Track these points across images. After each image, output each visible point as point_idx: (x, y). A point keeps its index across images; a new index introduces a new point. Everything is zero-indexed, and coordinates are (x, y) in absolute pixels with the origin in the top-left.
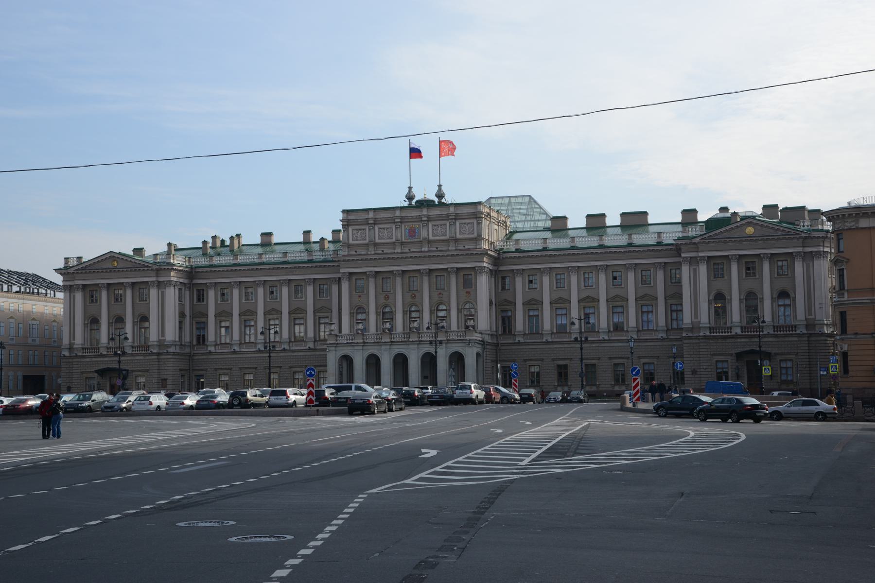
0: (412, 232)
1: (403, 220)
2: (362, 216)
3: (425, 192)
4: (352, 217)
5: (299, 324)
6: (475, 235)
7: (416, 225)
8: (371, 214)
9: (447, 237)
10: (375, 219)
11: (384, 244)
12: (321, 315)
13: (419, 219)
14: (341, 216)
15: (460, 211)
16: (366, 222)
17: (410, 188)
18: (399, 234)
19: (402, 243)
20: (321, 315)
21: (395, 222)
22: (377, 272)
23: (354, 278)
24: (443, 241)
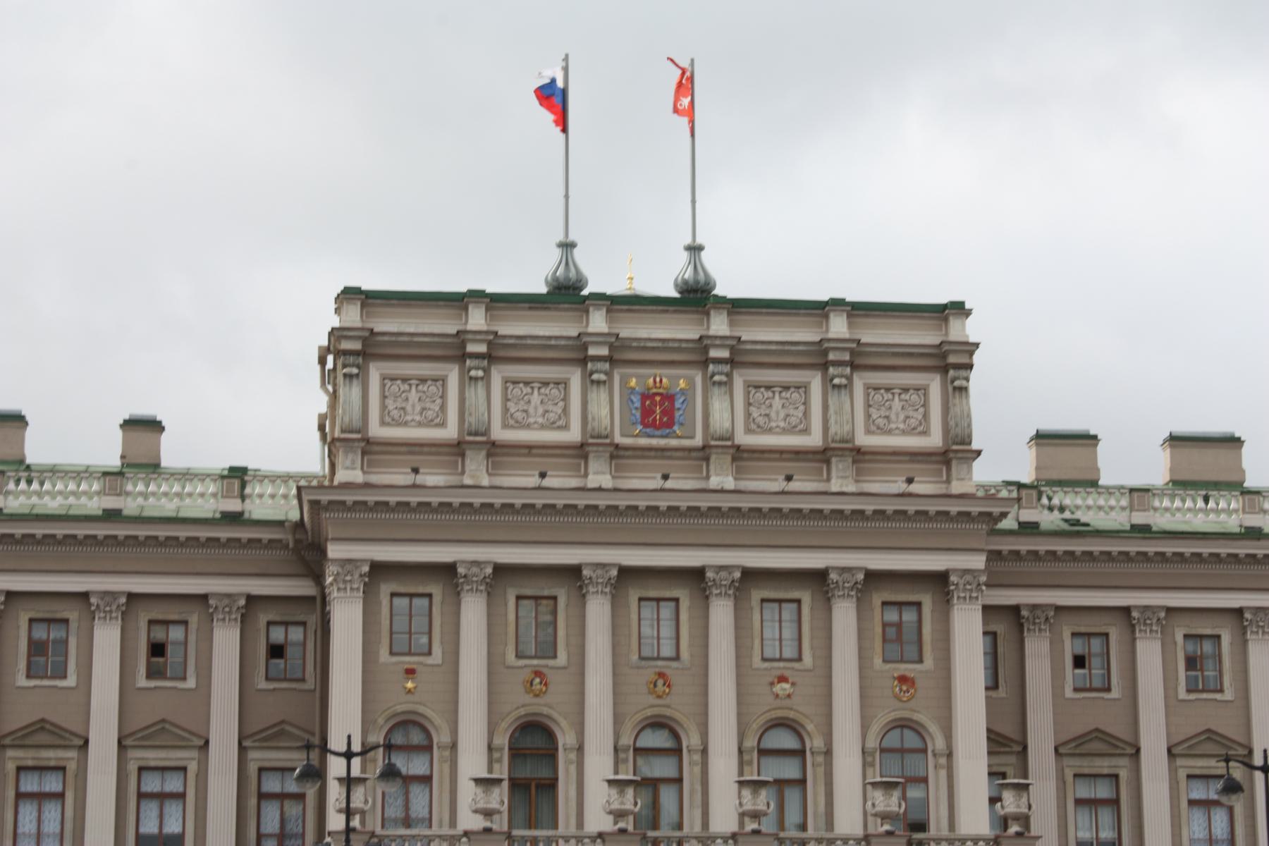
0: (658, 411)
1: (620, 353)
2: (441, 324)
3: (633, 261)
4: (388, 324)
5: (40, 797)
6: (934, 440)
7: (679, 380)
8: (477, 319)
9: (814, 439)
10: (494, 341)
11: (529, 449)
12: (154, 757)
13: (698, 354)
14: (324, 319)
15: (876, 334)
16: (454, 349)
17: (567, 246)
18: (606, 409)
19: (618, 454)
20: (154, 757)
21: (583, 361)
22: (501, 570)
23: (386, 589)
24: (798, 454)
